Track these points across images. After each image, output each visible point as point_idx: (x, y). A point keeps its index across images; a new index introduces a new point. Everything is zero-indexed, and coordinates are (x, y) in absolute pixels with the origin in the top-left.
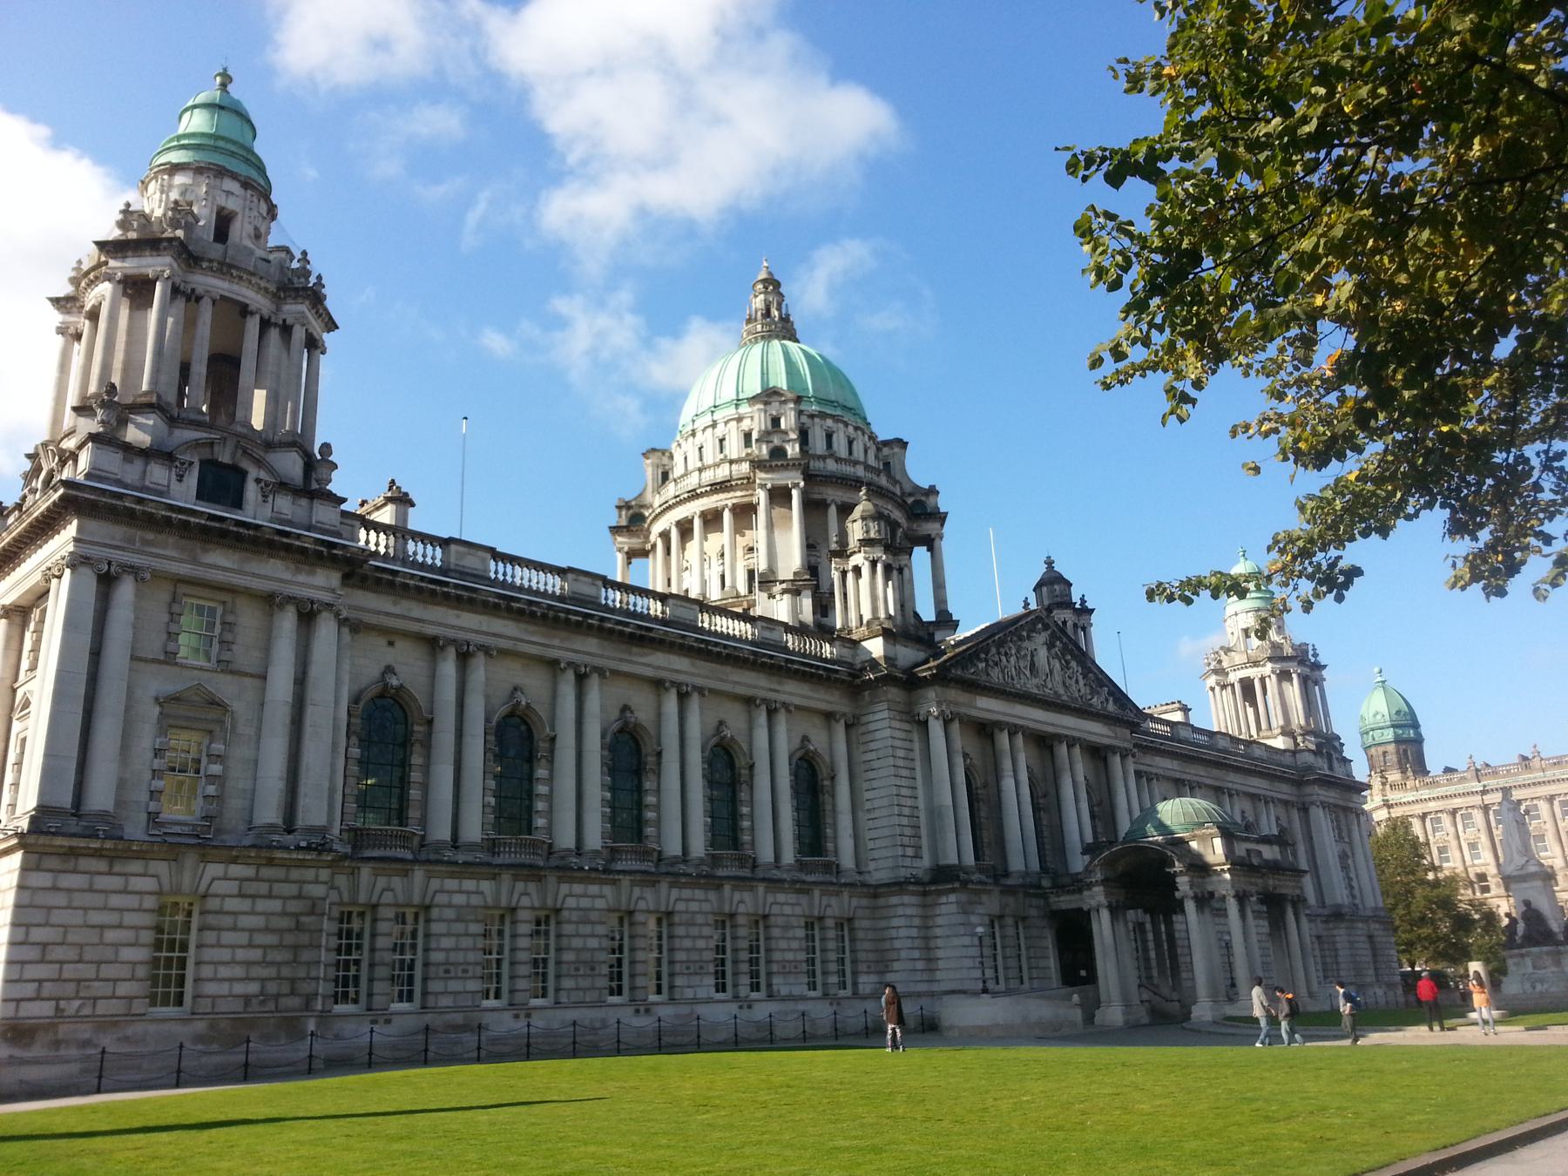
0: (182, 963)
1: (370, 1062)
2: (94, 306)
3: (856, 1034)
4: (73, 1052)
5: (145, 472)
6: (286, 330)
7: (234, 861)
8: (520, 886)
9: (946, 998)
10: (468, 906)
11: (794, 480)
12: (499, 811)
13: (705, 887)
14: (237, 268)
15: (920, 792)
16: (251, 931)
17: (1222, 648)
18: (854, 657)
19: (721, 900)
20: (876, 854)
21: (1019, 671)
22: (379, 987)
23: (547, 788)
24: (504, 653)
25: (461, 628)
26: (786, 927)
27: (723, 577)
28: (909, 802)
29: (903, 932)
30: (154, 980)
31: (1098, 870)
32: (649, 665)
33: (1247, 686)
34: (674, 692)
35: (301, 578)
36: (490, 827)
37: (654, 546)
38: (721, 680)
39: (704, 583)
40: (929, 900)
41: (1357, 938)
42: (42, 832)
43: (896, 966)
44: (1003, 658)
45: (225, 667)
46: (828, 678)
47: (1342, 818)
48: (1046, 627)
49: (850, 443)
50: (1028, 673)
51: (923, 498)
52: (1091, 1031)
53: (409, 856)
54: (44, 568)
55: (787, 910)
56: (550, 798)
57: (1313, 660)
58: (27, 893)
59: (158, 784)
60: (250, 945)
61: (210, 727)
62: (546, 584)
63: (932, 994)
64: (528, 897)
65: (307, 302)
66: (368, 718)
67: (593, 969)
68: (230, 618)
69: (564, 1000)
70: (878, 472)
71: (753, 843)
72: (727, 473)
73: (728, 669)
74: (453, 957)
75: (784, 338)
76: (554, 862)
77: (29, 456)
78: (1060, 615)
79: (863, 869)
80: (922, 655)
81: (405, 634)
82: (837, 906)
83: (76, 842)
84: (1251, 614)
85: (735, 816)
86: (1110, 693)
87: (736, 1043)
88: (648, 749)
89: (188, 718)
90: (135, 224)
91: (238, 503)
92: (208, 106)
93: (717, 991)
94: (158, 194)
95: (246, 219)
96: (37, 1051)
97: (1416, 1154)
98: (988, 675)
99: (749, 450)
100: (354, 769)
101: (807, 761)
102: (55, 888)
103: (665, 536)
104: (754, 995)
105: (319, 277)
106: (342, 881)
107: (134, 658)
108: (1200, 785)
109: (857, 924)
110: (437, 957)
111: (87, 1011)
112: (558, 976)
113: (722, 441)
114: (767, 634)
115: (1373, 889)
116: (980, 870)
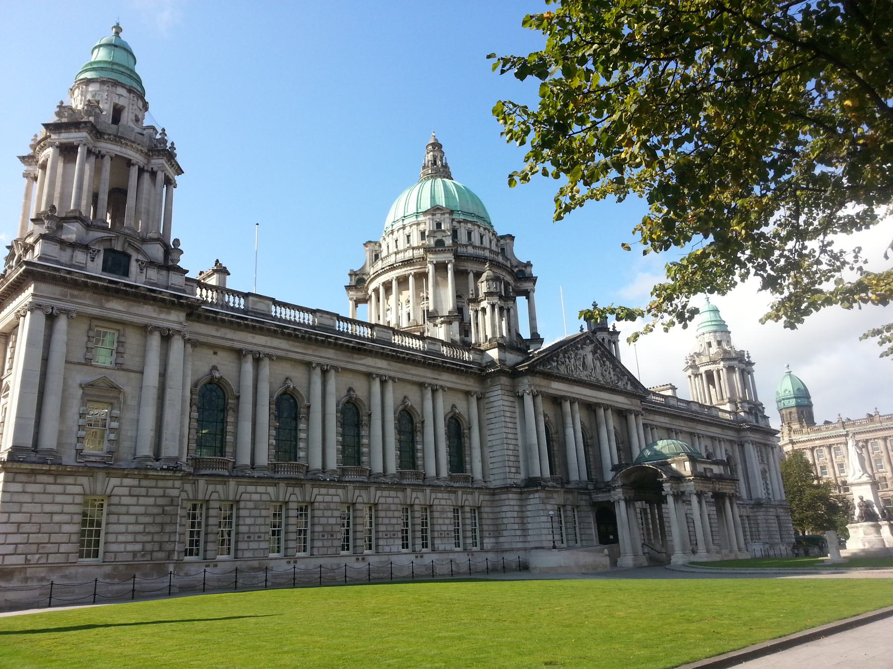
0: (98, 533)
1: (204, 588)
2: (43, 161)
3: (482, 572)
4: (35, 584)
5: (72, 256)
6: (153, 174)
7: (126, 476)
8: (290, 489)
9: (533, 551)
10: (261, 500)
11: (448, 257)
12: (278, 448)
13: (396, 490)
14: (125, 139)
15: (519, 436)
16: (137, 515)
17: (695, 353)
18: (481, 359)
19: (405, 497)
20: (494, 471)
21: (576, 367)
22: (210, 546)
23: (305, 435)
24: (280, 358)
25: (255, 344)
26: (443, 512)
27: (409, 314)
28: (513, 442)
29: (509, 514)
30: (82, 543)
31: (619, 479)
32: (363, 365)
33: (710, 376)
34: (378, 380)
35: (163, 316)
36: (273, 457)
37: (370, 297)
38: (405, 373)
39: (398, 318)
40: (524, 496)
41: (770, 517)
42: (15, 461)
43: (505, 533)
44: (567, 360)
45: (119, 366)
46: (467, 372)
47: (763, 450)
48: (592, 342)
49: (482, 237)
50: (581, 368)
51: (523, 269)
52: (614, 570)
53: (227, 473)
54: (16, 311)
55: (443, 502)
56: (307, 440)
57: (747, 360)
58: (8, 495)
59: (82, 433)
60: (137, 523)
61: (112, 401)
62: (304, 319)
63: (525, 549)
64: (295, 496)
65: (165, 158)
66: (202, 396)
67: (332, 536)
68: (122, 339)
69: (315, 553)
70: (497, 254)
71: (424, 465)
72: (411, 255)
73: (409, 367)
74: (252, 529)
75: (444, 177)
76: (309, 476)
77: (8, 247)
78: (600, 335)
79: (487, 480)
80: (520, 359)
81: (224, 348)
82: (470, 500)
83: (34, 467)
84: (711, 334)
85: (413, 451)
86: (629, 380)
87: (413, 578)
88: (363, 412)
89: (99, 396)
90: (66, 115)
91: (126, 274)
92: (108, 45)
93: (403, 548)
94: (80, 96)
95: (130, 111)
96: (15, 583)
97: (765, 640)
98: (558, 369)
99: (424, 242)
100: (195, 424)
101: (455, 419)
102: (24, 492)
103: (376, 291)
104: (424, 550)
105: (173, 144)
106: (188, 487)
107: (67, 362)
108: (681, 432)
109: (483, 510)
110: (243, 529)
111: (43, 561)
112: (312, 540)
113: (408, 236)
114: (432, 347)
115: (780, 490)
116: (553, 480)
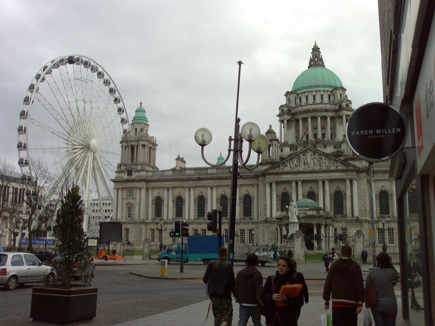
34: (209, 188)
44: (291, 164)
51: (341, 104)
